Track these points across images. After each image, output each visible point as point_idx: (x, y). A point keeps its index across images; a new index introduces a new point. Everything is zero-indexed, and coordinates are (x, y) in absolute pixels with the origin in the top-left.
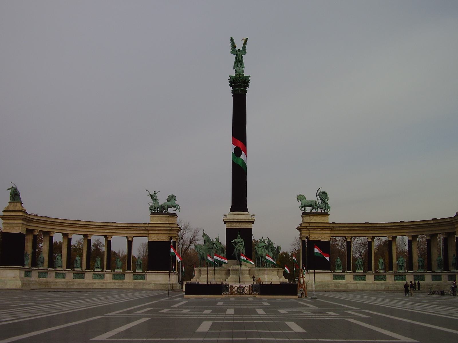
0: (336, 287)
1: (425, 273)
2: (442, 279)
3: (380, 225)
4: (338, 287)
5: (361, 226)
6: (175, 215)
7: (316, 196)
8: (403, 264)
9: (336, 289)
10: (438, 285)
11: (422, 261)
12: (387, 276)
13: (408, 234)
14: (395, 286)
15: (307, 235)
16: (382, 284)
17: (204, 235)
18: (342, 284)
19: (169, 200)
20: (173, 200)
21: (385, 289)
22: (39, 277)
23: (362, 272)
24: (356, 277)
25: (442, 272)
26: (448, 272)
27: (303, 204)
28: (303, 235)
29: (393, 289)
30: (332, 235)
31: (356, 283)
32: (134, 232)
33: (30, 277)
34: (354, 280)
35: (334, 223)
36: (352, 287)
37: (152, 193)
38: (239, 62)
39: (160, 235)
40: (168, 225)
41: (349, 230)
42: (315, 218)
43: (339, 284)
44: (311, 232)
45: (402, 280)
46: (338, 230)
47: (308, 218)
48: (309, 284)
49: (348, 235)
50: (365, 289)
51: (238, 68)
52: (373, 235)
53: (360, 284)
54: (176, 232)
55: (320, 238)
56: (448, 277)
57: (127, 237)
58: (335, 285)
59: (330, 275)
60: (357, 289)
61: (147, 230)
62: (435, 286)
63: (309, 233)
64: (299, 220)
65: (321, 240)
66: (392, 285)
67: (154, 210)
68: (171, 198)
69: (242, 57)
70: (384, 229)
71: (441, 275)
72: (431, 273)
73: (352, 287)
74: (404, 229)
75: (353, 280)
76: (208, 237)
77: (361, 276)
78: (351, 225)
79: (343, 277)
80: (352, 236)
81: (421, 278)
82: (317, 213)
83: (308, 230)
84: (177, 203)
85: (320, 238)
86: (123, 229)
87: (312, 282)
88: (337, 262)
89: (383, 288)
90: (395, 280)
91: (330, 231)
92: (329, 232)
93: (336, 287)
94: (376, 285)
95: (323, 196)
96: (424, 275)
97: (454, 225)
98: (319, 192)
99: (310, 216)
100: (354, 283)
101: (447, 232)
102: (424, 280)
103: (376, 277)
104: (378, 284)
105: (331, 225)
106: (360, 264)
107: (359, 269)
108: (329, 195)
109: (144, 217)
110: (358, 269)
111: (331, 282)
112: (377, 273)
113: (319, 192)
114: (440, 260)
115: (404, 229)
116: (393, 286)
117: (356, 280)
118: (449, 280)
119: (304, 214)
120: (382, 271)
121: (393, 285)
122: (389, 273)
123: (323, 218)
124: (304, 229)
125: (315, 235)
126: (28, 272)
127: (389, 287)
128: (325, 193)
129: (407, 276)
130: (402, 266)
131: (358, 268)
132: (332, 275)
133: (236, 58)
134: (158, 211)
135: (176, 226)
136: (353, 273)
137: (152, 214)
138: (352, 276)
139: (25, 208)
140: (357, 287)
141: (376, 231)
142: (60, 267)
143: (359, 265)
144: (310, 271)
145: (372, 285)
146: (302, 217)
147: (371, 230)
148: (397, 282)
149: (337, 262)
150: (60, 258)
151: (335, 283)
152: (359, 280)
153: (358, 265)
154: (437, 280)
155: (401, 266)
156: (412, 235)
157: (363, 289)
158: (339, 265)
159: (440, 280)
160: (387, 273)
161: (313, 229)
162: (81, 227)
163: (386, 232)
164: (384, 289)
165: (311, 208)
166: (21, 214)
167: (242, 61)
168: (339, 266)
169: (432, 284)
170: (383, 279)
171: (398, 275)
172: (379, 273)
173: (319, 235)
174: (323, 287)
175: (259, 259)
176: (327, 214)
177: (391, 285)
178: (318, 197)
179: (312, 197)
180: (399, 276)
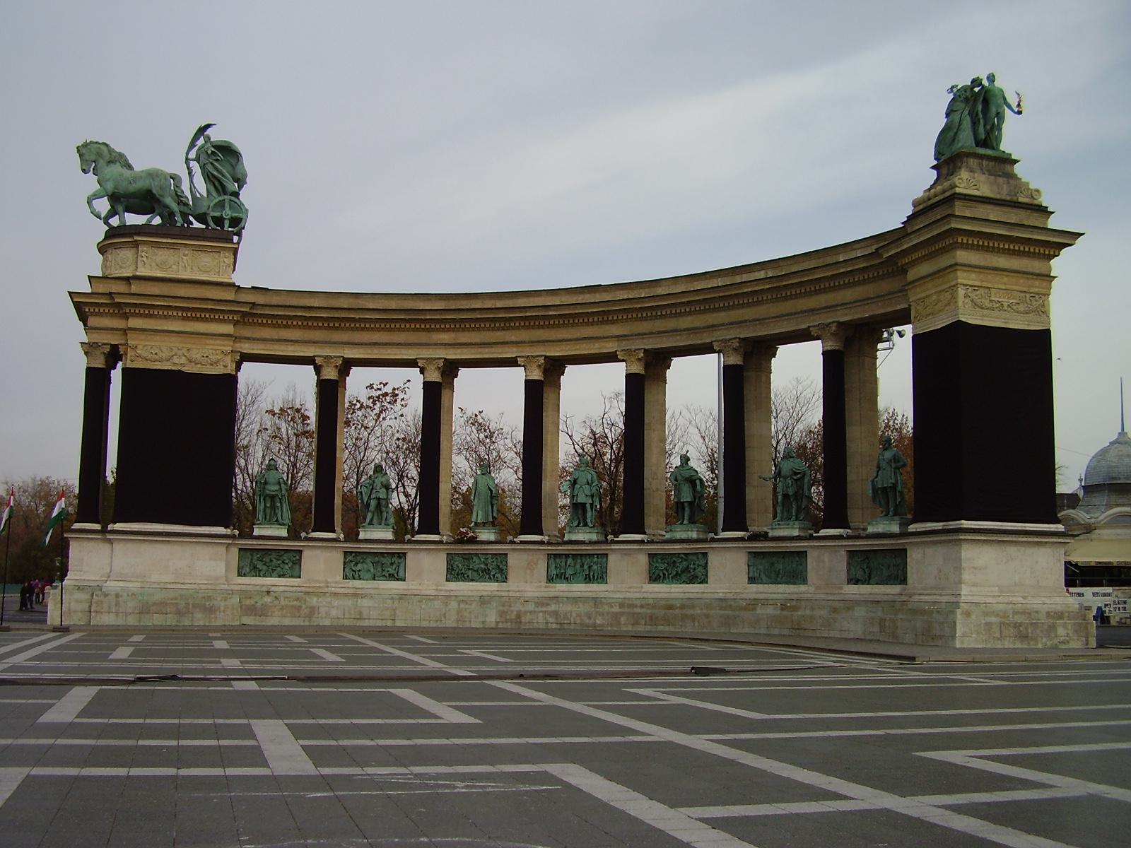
0: (251, 610)
1: (714, 545)
2: (812, 575)
3: (489, 304)
4: (262, 612)
5: (393, 304)
7: (187, 159)
8: (592, 496)
9: (248, 620)
12: (513, 560)
13: (625, 345)
14: (553, 607)
15: (114, 340)
16: (484, 600)
18: (282, 599)
21: (500, 625)
23: (389, 535)
24: (355, 564)
25: (811, 538)
26: (849, 537)
27: (110, 186)
29: (541, 626)
31: (355, 595)
34: (345, 577)
36: (334, 613)
42: (162, 255)
43: (267, 599)
44: (134, 323)
45: (588, 579)
47: (127, 254)
48: (106, 595)
50: (399, 623)
52: (453, 355)
53: (376, 598)
55: (183, 360)
56: (849, 564)
58: (248, 602)
59: (223, 550)
60: (360, 623)
62: (770, 610)
63: (125, 331)
65: (185, 369)
66: (537, 604)
71: (802, 555)
73: (331, 612)
75: (339, 578)
77: (384, 560)
78: (344, 303)
79: (286, 562)
81: (687, 569)
85: (183, 360)
87: (121, 584)
88: (266, 483)
89: (492, 618)
90: (550, 579)
91: (236, 323)
92: (228, 329)
93: (251, 610)
94: (454, 604)
95: (221, 161)
96: (705, 554)
97: (904, 271)
99: (136, 245)
100: (345, 595)
101: (842, 320)
102: (704, 581)
104: (463, 600)
106: (379, 499)
107: (375, 521)
108: (249, 163)
110: (371, 523)
111: (226, 587)
112: (460, 541)
113: (201, 141)
114: (796, 474)
116: (540, 609)
117: (354, 578)
118: (853, 581)
119: (115, 238)
120: (486, 535)
121: (542, 602)
122: (522, 542)
123: (206, 260)
125: (157, 341)
127: (519, 616)
128: (227, 152)
129: (613, 559)
131: (369, 516)
132: (235, 552)
136: (346, 541)
138: (338, 557)
140: (361, 613)
141: (466, 334)
143: (373, 503)
144: (119, 526)
145: (437, 604)
146: (102, 249)
148: (561, 587)
149: (266, 483)
151: (245, 595)
152: (370, 576)
153: (368, 505)
154: (776, 577)
155: (585, 511)
156: (646, 351)
157: (389, 623)
158: (273, 498)
159: (798, 576)
160: (514, 543)
161: (147, 310)
163: (513, 339)
164: (493, 625)
168: (273, 507)
169: (753, 604)
170: (487, 571)
171: (567, 556)
172: (473, 541)
173: (175, 343)
174: (180, 613)
177: (531, 607)
180: (570, 561)
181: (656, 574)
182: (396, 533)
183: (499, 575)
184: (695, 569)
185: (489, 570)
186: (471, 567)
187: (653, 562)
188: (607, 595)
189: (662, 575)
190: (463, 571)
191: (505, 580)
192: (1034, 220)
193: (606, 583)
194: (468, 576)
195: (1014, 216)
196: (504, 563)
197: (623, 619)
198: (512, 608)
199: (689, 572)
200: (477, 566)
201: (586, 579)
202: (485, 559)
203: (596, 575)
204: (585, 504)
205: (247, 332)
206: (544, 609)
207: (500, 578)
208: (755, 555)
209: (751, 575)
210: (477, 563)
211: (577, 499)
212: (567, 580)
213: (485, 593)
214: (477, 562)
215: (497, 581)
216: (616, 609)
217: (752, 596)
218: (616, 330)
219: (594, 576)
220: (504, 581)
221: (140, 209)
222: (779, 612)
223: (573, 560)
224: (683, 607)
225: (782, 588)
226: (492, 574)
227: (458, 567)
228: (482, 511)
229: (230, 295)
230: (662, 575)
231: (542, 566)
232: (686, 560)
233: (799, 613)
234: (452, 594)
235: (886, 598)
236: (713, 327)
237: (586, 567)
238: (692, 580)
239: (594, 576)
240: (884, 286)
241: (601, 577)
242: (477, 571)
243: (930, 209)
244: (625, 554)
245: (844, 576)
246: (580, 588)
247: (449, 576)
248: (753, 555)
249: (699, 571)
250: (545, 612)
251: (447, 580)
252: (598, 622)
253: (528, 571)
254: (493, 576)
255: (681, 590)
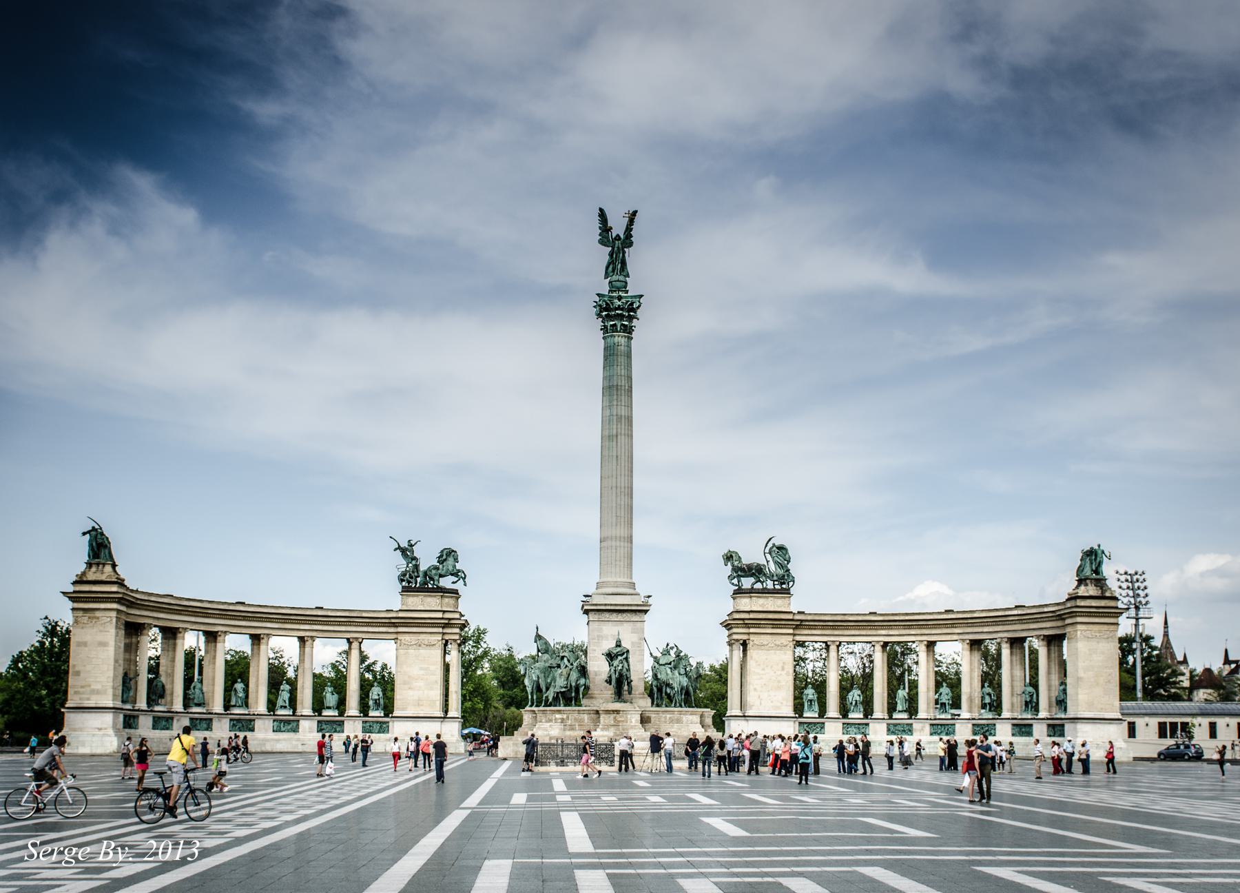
6: (455, 592)
11: (989, 694)
12: (915, 726)
15: (745, 637)
17: (538, 637)
19: (442, 560)
20: (451, 560)
22: (154, 728)
28: (735, 637)
30: (798, 638)
32: (365, 629)
33: (136, 728)
35: (803, 613)
37: (404, 544)
38: (617, 265)
39: (422, 637)
40: (440, 615)
41: (833, 628)
42: (761, 601)
44: (752, 630)
46: (810, 627)
49: (832, 639)
51: (615, 278)
54: (457, 630)
57: (348, 639)
61: (394, 625)
64: (727, 606)
67: (409, 582)
68: (448, 555)
69: (624, 253)
70: (910, 627)
76: (546, 643)
80: (842, 639)
82: (765, 591)
83: (747, 626)
84: (458, 566)
86: (340, 624)
92: (791, 631)
98: (770, 545)
103: (892, 728)
105: (797, 617)
109: (386, 596)
113: (770, 545)
115: (953, 625)
119: (739, 592)
123: (779, 602)
124: (737, 626)
126: (130, 716)
128: (781, 548)
129: (957, 726)
133: (611, 255)
134: (416, 581)
135: (457, 616)
137: (406, 590)
139: (122, 576)
142: (198, 705)
147: (882, 627)
150: (199, 685)
162: (245, 618)
165: (752, 580)
166: (114, 588)
167: (624, 263)
175: (660, 690)
176: (787, 592)
178: (768, 556)
179: (753, 554)
192: (1112, 603)
195: (1103, 603)
205: (797, 632)
208: (1014, 725)
221: (744, 572)
229: (790, 617)
231: (927, 728)
240: (1059, 623)
243: (1073, 598)
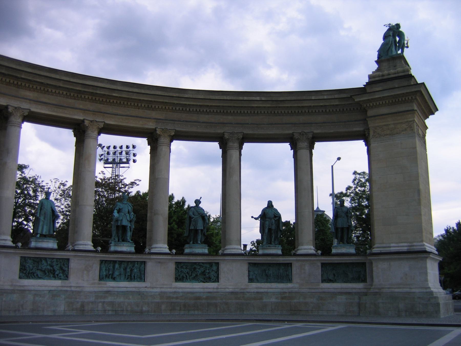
2: (296, 278)
10: (283, 295)
14: (110, 299)
16: (54, 294)
45: (130, 278)
56: (322, 270)
62: (273, 300)
72: (246, 258)
74: (148, 108)
81: (203, 273)
102: (217, 280)
103: (30, 265)
104: (37, 293)
116: (99, 300)
127: (83, 306)
130: (128, 227)
148: (111, 284)
163: (81, 107)
171: (115, 262)
177: (92, 299)
180: (117, 266)
181: (181, 276)
182: (282, 250)
183: (61, 274)
184: (209, 273)
185: (54, 270)
186: (40, 268)
187: (178, 267)
188: (147, 290)
189: (185, 276)
190: (34, 271)
191: (67, 277)
193: (144, 281)
194: (37, 275)
196: (66, 265)
197: (163, 307)
198: (78, 300)
199: (205, 275)
200: (45, 267)
201: (128, 278)
202: (51, 262)
203: (136, 276)
204: (127, 226)
206: (102, 300)
207: (62, 277)
209: (251, 277)
210: (45, 266)
211: (121, 223)
212: (114, 279)
213: (53, 289)
214: (45, 264)
215: (60, 279)
216: (157, 300)
217: (256, 290)
218: (154, 114)
219: (134, 277)
220: (66, 279)
222: (279, 301)
223: (119, 265)
224: (207, 298)
225: (274, 285)
226: (56, 273)
227: (29, 267)
228: (47, 226)
230: (185, 276)
231: (96, 267)
232: (203, 267)
233: (295, 301)
234: (26, 288)
235: (354, 291)
236: (224, 124)
237: (128, 270)
238: (208, 279)
239: (134, 277)
241: (141, 277)
242: (44, 271)
244: (159, 262)
245: (320, 278)
246: (124, 285)
247: (21, 274)
248: (251, 265)
249: (213, 274)
250: (104, 302)
251: (20, 278)
252: (144, 309)
253: (85, 272)
254: (57, 275)
255: (201, 287)
